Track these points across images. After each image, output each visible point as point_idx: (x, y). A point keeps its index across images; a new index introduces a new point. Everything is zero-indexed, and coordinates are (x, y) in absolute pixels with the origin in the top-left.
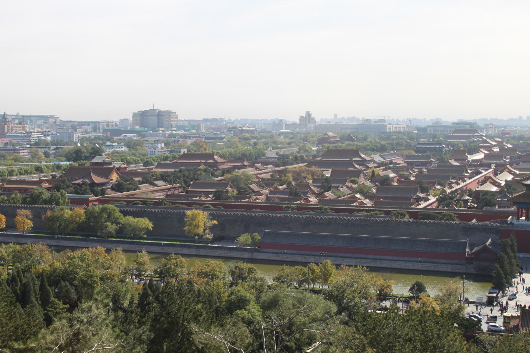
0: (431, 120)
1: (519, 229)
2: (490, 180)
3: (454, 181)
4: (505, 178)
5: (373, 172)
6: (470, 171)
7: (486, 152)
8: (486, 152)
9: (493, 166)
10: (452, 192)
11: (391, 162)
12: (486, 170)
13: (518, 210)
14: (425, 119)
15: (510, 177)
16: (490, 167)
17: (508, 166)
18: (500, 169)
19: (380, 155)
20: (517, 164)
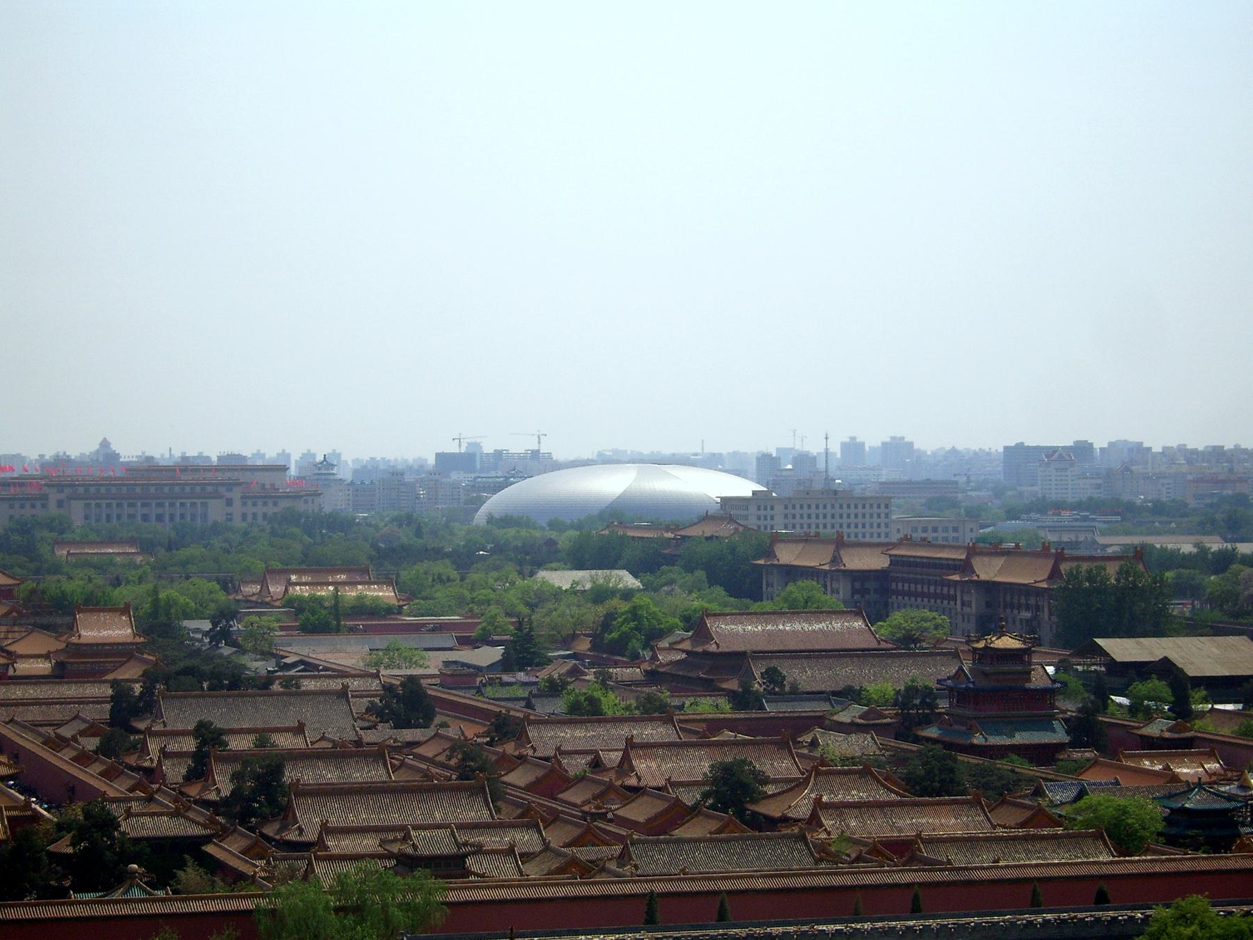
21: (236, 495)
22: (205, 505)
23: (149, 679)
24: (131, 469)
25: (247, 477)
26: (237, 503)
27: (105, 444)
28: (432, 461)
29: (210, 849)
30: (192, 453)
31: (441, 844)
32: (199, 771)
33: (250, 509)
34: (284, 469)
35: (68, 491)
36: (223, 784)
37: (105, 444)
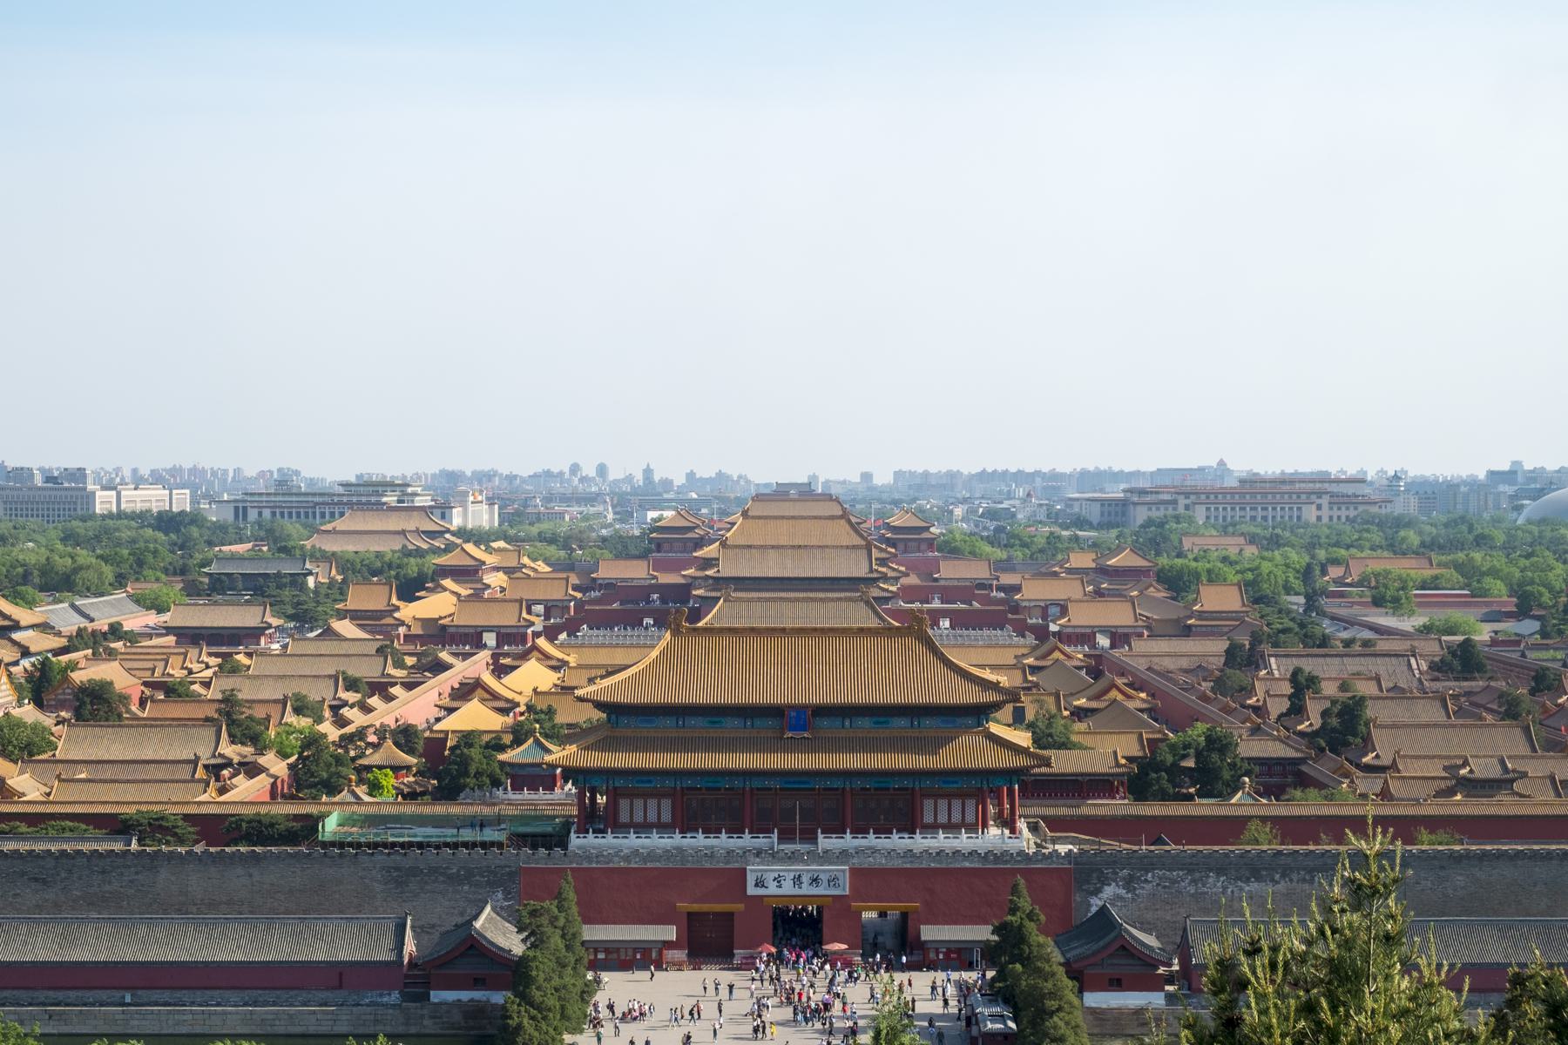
0: (262, 474)
1: (585, 865)
2: (480, 691)
3: (352, 697)
4: (530, 679)
5: (44, 666)
6: (410, 661)
7: (464, 592)
8: (464, 592)
9: (490, 639)
10: (347, 740)
11: (115, 631)
12: (466, 656)
13: (581, 795)
14: (237, 471)
15: (546, 679)
16: (480, 645)
17: (542, 642)
18: (513, 646)
19: (73, 606)
20: (572, 633)
21: (1325, 501)
22: (1299, 509)
23: (1256, 639)
24: (1243, 481)
25: (1334, 488)
26: (1325, 506)
27: (1222, 463)
28: (1482, 476)
29: (1304, 768)
30: (1289, 470)
31: (1483, 769)
32: (1297, 710)
33: (1336, 513)
34: (1363, 481)
35: (1193, 497)
36: (1312, 720)
37: (1222, 463)
